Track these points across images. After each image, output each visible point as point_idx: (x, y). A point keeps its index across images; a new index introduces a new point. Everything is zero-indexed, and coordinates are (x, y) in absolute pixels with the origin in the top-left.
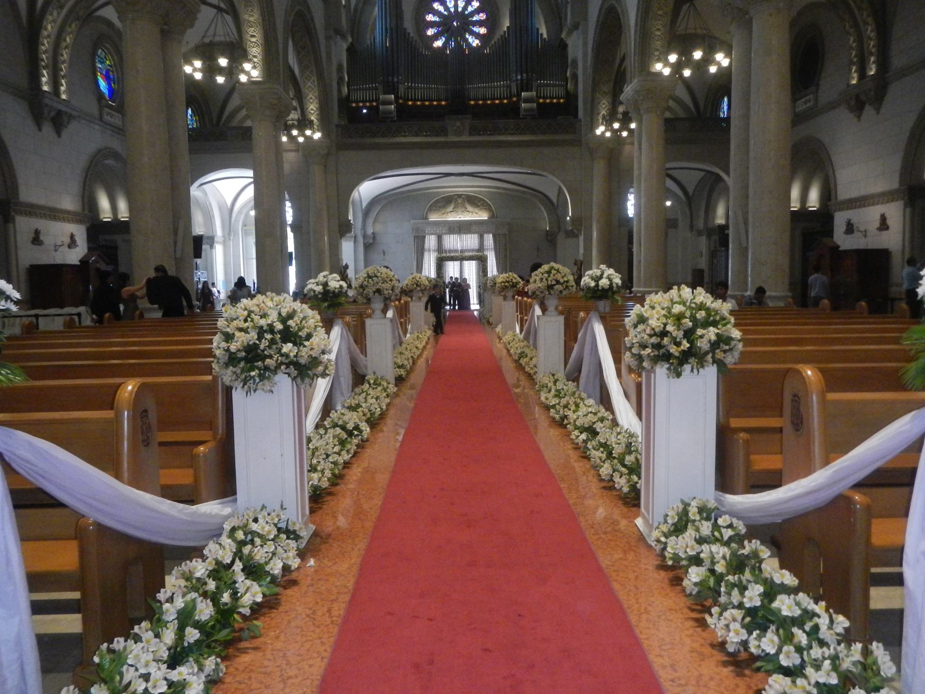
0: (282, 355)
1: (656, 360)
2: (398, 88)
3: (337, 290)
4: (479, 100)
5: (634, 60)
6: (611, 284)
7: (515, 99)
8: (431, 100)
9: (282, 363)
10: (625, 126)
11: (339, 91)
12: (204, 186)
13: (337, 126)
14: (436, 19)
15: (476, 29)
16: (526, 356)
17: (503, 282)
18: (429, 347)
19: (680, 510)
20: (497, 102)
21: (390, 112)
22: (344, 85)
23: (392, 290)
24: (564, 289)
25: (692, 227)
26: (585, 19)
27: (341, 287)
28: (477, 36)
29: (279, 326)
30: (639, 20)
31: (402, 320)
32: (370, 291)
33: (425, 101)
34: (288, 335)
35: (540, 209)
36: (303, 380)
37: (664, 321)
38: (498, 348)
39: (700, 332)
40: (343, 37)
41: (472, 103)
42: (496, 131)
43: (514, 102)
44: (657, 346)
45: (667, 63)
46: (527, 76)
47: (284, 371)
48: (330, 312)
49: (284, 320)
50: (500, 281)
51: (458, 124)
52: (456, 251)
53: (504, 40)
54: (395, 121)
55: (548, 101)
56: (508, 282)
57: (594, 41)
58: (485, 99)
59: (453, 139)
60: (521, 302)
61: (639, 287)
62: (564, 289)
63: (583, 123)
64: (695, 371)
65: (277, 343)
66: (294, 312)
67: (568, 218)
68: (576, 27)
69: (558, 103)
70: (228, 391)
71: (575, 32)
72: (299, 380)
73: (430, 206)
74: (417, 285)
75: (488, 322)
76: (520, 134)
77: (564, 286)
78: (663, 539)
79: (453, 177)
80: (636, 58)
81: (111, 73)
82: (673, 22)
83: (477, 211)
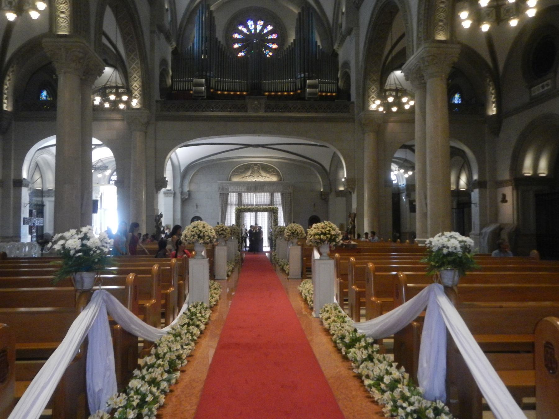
2: (210, 80)
4: (272, 92)
7: (299, 91)
8: (235, 91)
13: (157, 101)
17: (317, 234)
20: (285, 93)
21: (201, 92)
26: (358, 26)
28: (271, 49)
40: (168, 38)
42: (286, 109)
43: (299, 94)
46: (309, 75)
50: (312, 233)
51: (256, 102)
52: (253, 205)
53: (292, 49)
54: (205, 99)
56: (325, 234)
57: (366, 38)
58: (276, 92)
63: (355, 105)
71: (348, 37)
73: (233, 172)
74: (199, 237)
75: (283, 270)
79: (251, 148)
83: (268, 176)
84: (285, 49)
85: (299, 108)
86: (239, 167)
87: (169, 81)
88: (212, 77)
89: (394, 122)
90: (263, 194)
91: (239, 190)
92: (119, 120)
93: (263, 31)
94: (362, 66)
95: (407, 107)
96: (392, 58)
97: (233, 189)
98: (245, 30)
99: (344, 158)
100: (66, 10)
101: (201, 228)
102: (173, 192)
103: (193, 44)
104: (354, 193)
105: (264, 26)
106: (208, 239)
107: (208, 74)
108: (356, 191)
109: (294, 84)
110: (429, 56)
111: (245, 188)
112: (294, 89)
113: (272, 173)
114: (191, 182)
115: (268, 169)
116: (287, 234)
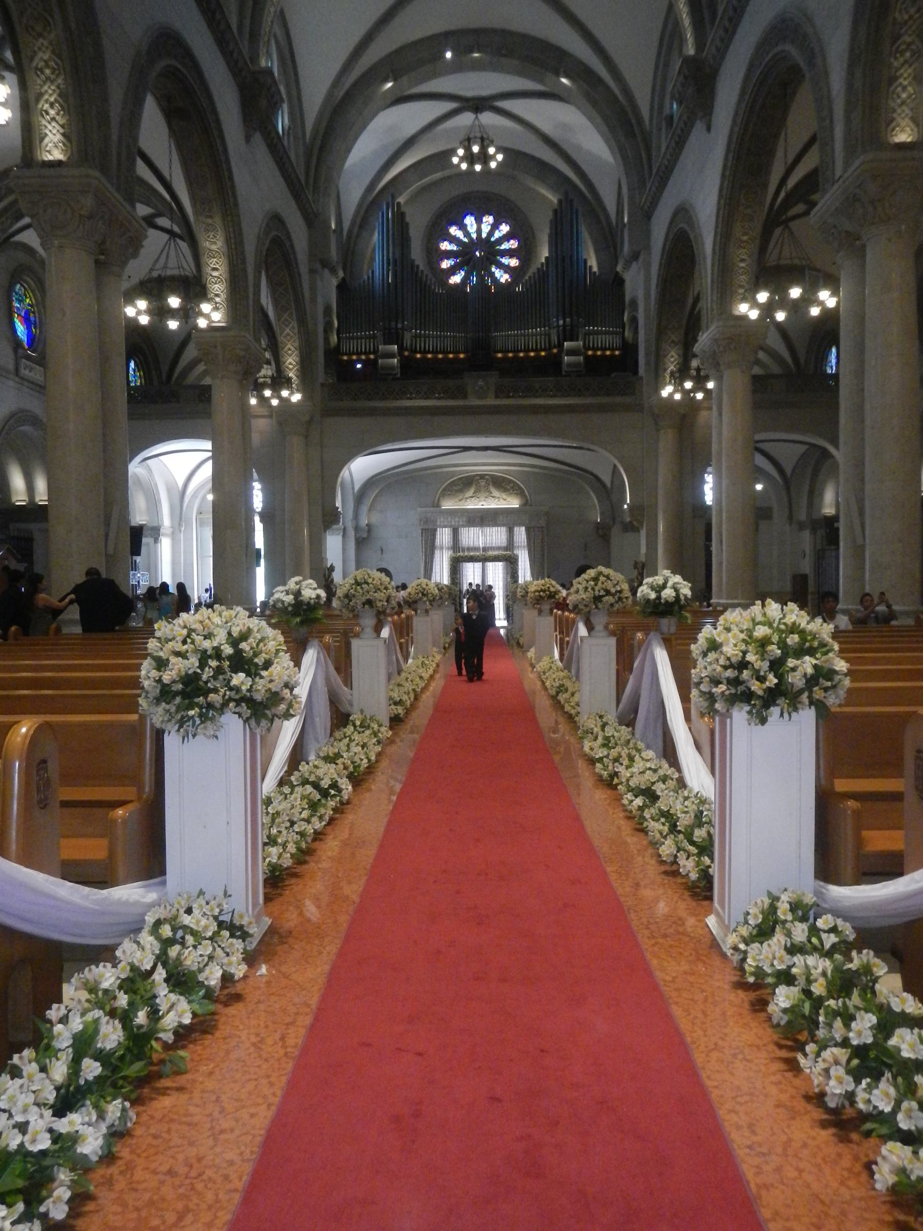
0: (231, 689)
1: (732, 700)
2: (403, 333)
3: (312, 601)
4: (509, 352)
5: (712, 301)
6: (677, 597)
7: (555, 351)
8: (445, 352)
9: (231, 699)
10: (700, 382)
11: (327, 339)
12: (149, 462)
13: (322, 385)
14: (453, 247)
15: (505, 261)
16: (567, 690)
17: (536, 591)
18: (437, 676)
19: (766, 906)
20: (532, 354)
21: (392, 368)
23: (388, 601)
24: (617, 602)
25: (790, 518)
26: (648, 248)
27: (318, 597)
28: (506, 269)
29: (228, 650)
30: (717, 248)
31: (402, 640)
32: (358, 602)
33: (437, 353)
34: (240, 662)
36: (258, 723)
37: (743, 647)
38: (530, 679)
39: (791, 662)
40: (333, 271)
41: (500, 355)
42: (530, 392)
43: (555, 355)
44: (735, 682)
45: (755, 304)
46: (571, 321)
47: (233, 710)
48: (304, 630)
49: (234, 642)
50: (533, 590)
51: (481, 383)
52: (476, 549)
53: (542, 274)
54: (398, 379)
55: (599, 353)
56: (544, 591)
57: (659, 276)
58: (516, 351)
59: (474, 402)
60: (561, 618)
61: (720, 598)
62: (617, 602)
64: (786, 715)
65: (224, 673)
66: (249, 630)
67: (626, 506)
68: (635, 256)
69: (613, 356)
70: (159, 736)
71: (634, 264)
72: (253, 722)
73: (444, 490)
74: (423, 594)
75: (518, 643)
76: (563, 396)
77: (616, 597)
78: (742, 946)
79: (474, 452)
80: (715, 298)
81: (32, 315)
82: (763, 249)
83: (505, 497)
87: (334, 339)
91: (453, 523)
93: (493, 235)
98: (459, 234)
99: (625, 471)
105: (495, 226)
107: (400, 326)
110: (724, 340)
111: (464, 519)
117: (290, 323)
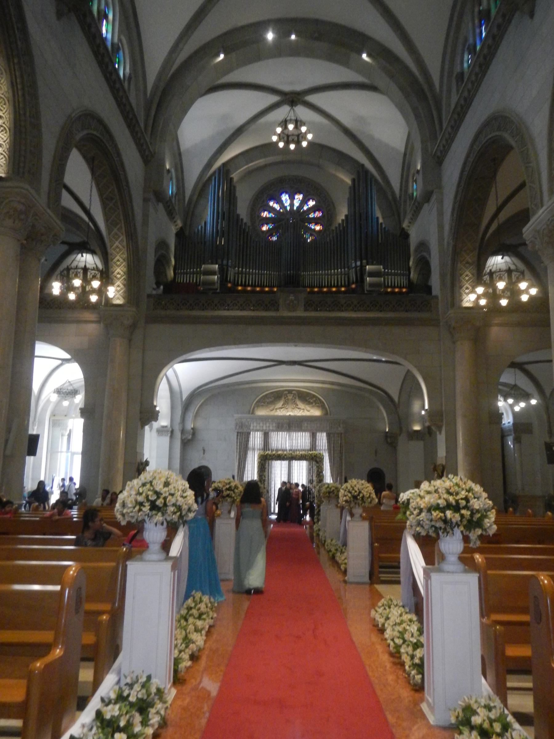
7: (353, 286)
13: (149, 296)
14: (271, 215)
17: (437, 507)
21: (213, 283)
22: (169, 267)
26: (440, 187)
35: (378, 408)
40: (171, 214)
51: (292, 297)
53: (344, 229)
56: (456, 508)
58: (321, 287)
59: (285, 313)
68: (427, 197)
71: (426, 207)
73: (257, 402)
74: (154, 507)
76: (365, 310)
79: (284, 367)
83: (308, 408)
84: (333, 228)
85: (356, 306)
86: (266, 395)
88: (231, 267)
89: (500, 325)
90: (300, 434)
91: (264, 428)
92: (92, 322)
94: (448, 243)
95: (525, 298)
96: (500, 227)
97: (256, 426)
98: (277, 207)
100: (4, 142)
101: (159, 487)
102: (171, 429)
103: (205, 223)
104: (440, 433)
105: (304, 202)
106: (174, 513)
108: (443, 432)
109: (346, 276)
111: (274, 425)
112: (347, 283)
113: (314, 404)
114: (196, 415)
115: (308, 398)
116: (345, 498)
117: (119, 237)
